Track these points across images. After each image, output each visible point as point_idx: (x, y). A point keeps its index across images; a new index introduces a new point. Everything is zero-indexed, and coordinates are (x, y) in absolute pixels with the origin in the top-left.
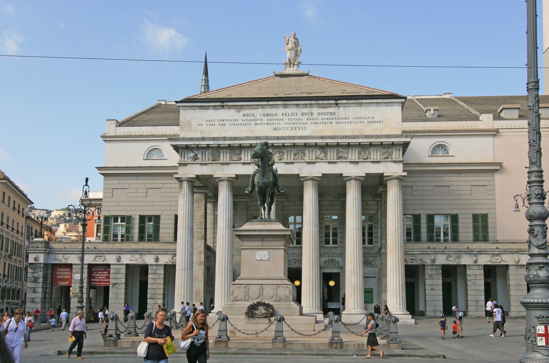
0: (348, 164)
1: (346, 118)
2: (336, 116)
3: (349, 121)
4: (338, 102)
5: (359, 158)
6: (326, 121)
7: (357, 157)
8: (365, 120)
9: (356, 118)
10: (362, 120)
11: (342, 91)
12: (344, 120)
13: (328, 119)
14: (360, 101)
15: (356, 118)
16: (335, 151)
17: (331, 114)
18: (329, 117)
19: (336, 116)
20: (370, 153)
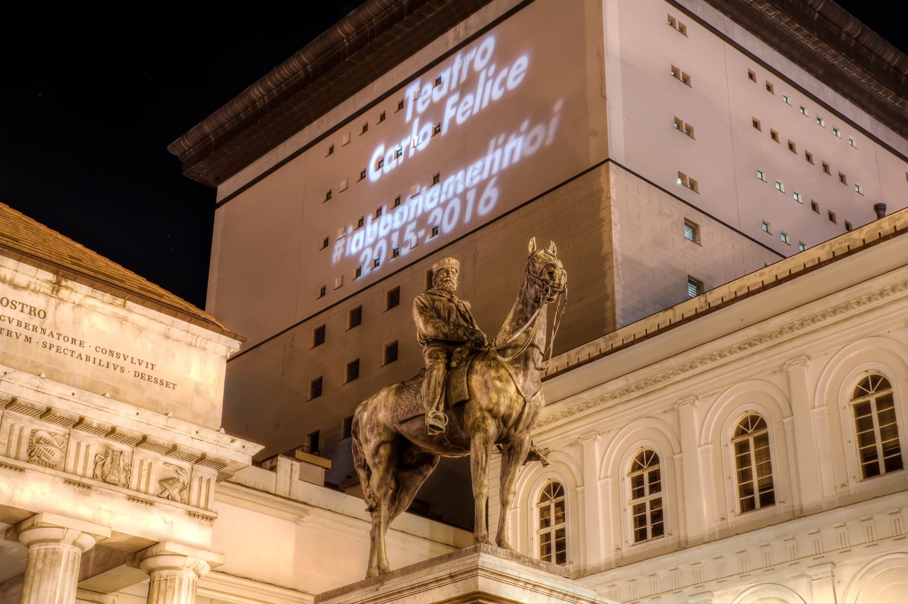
0: (62, 486)
1: (74, 341)
2: (48, 323)
3: (85, 351)
4: (63, 283)
5: (94, 477)
6: (13, 327)
7: (90, 473)
8: (127, 364)
9: (104, 351)
10: (120, 362)
11: (71, 257)
12: (69, 346)
13: (19, 324)
14: (129, 304)
15: (104, 351)
16: (27, 433)
17: (33, 311)
18: (24, 317)
19: (48, 323)
20: (128, 471)
